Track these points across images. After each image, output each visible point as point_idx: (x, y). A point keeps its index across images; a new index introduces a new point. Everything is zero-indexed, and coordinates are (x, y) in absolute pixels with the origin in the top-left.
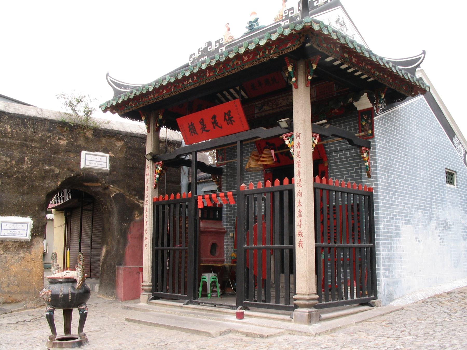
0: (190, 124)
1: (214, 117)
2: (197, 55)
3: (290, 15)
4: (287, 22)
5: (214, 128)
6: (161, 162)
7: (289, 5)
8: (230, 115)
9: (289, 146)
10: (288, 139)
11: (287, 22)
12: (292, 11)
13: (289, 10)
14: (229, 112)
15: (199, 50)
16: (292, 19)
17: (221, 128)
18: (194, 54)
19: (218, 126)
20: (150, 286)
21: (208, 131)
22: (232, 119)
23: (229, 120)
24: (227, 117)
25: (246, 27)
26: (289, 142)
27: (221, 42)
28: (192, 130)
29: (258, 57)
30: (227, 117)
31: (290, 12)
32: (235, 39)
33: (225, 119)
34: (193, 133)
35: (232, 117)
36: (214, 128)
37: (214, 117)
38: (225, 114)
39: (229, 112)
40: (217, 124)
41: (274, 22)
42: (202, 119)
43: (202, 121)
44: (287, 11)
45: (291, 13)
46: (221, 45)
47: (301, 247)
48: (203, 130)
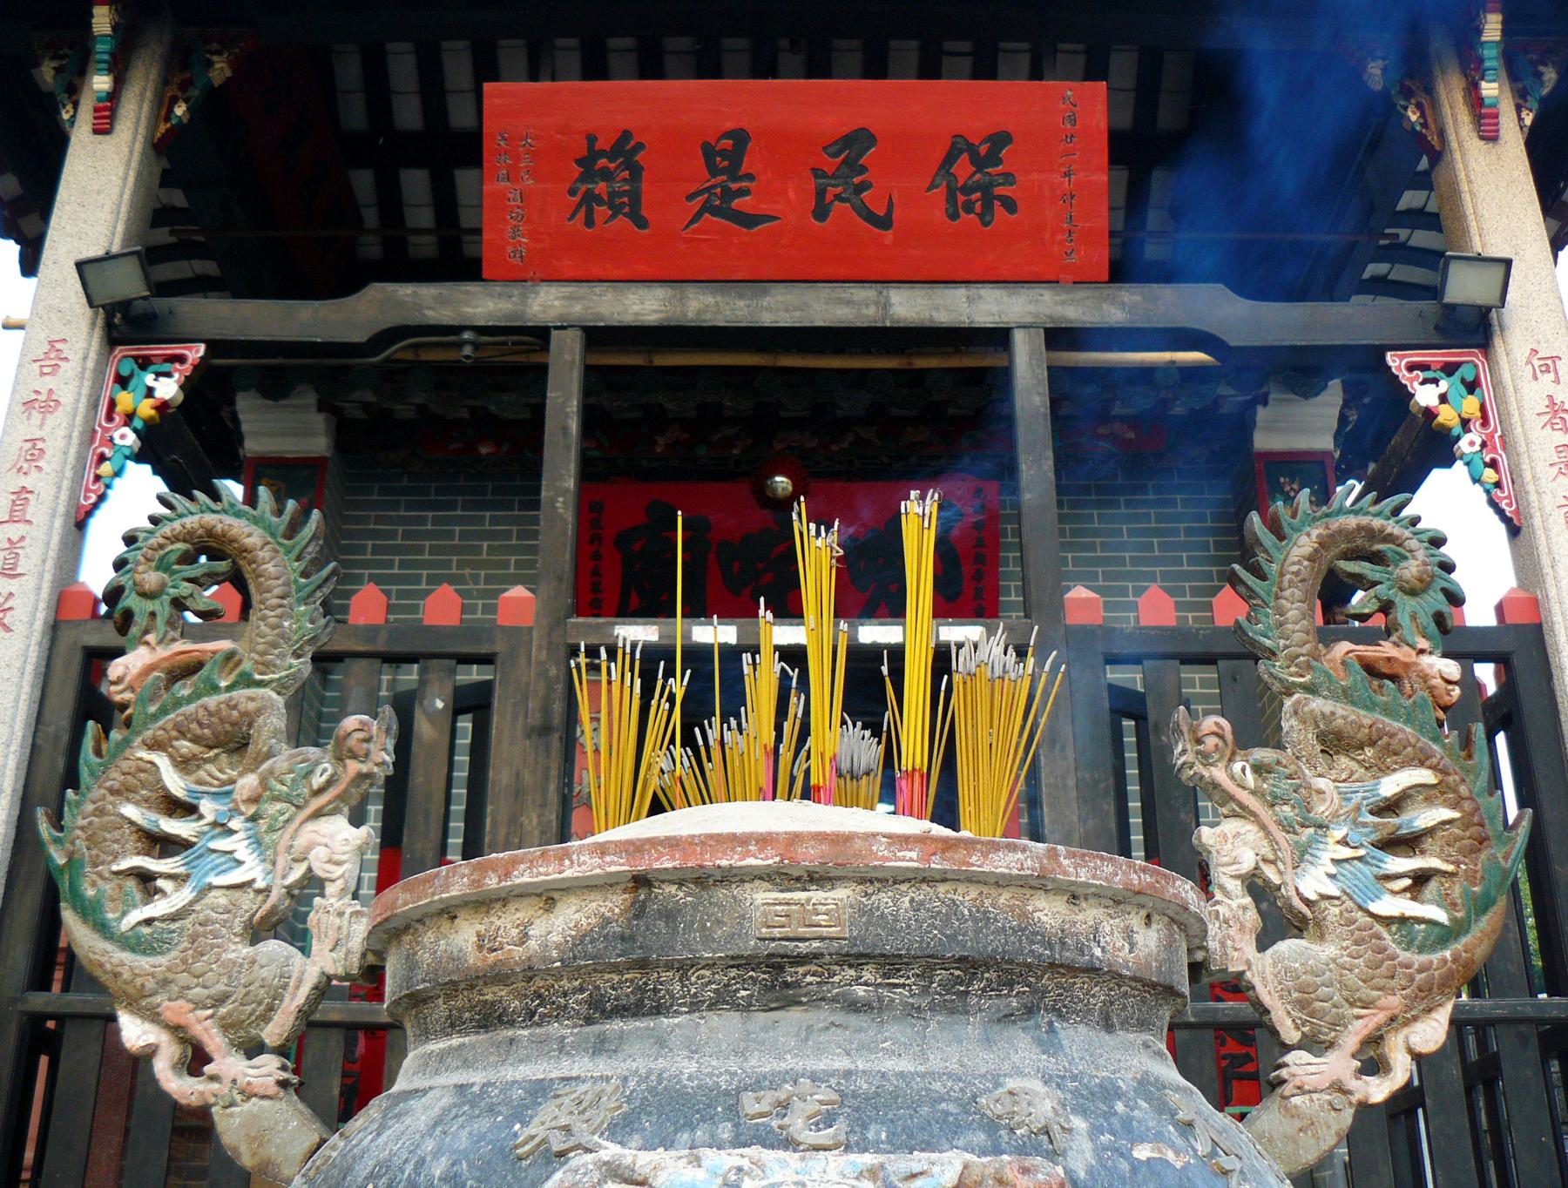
0: (602, 144)
5: (821, 213)
6: (196, 352)
8: (993, 158)
9: (1447, 416)
10: (1435, 381)
14: (1000, 139)
17: (884, 223)
26: (1443, 398)
34: (601, 210)
35: (1008, 177)
36: (821, 213)
37: (856, 141)
39: (1000, 139)
42: (740, 137)
43: (727, 143)
48: (706, 208)
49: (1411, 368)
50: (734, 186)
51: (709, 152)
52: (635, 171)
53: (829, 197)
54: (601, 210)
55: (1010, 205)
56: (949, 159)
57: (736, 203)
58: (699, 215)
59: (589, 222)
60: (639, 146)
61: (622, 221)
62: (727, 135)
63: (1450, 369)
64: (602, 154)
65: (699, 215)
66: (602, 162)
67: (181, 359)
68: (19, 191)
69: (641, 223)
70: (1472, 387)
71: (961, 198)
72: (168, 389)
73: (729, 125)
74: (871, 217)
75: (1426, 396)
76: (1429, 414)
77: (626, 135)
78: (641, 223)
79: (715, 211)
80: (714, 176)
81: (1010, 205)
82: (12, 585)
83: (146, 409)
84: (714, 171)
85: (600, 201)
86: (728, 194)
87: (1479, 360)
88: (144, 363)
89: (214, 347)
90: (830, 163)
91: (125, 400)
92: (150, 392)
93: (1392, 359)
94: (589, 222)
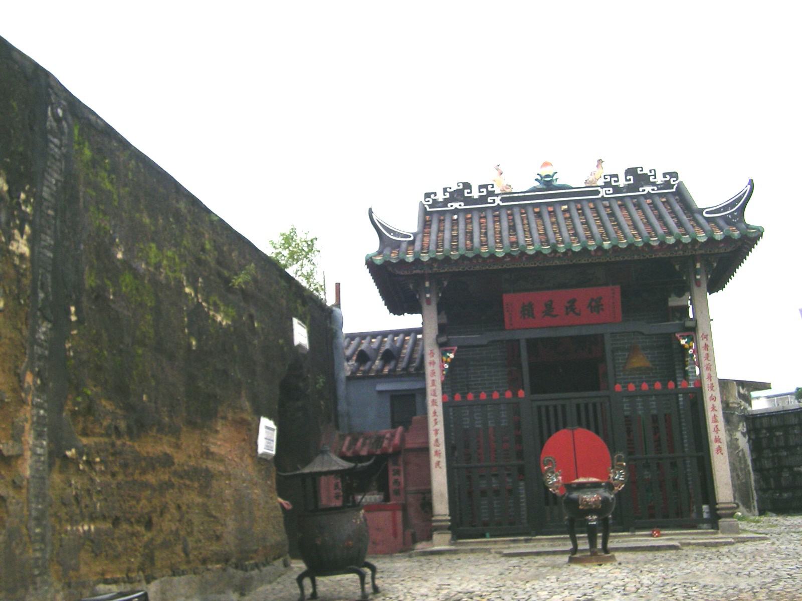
1: (573, 301)
2: (440, 197)
3: (613, 183)
4: (609, 191)
5: (567, 314)
6: (456, 348)
7: (608, 169)
9: (687, 346)
11: (609, 191)
12: (616, 179)
13: (612, 176)
15: (445, 190)
16: (617, 189)
18: (435, 194)
20: (449, 521)
24: (594, 304)
25: (536, 180)
26: (686, 342)
27: (490, 189)
28: (526, 312)
29: (676, 248)
30: (594, 304)
31: (613, 179)
32: (513, 191)
35: (602, 305)
36: (567, 314)
38: (593, 299)
39: (601, 298)
41: (584, 186)
44: (608, 177)
45: (615, 181)
46: (491, 194)
47: (720, 454)
49: (680, 336)
51: (546, 305)
54: (526, 316)
55: (602, 309)
63: (688, 336)
67: (453, 350)
70: (692, 340)
72: (452, 356)
74: (577, 314)
75: (683, 342)
76: (683, 346)
78: (534, 318)
81: (602, 309)
82: (436, 398)
83: (449, 360)
87: (694, 335)
88: (447, 351)
89: (459, 347)
91: (445, 359)
92: (449, 357)
93: (677, 335)
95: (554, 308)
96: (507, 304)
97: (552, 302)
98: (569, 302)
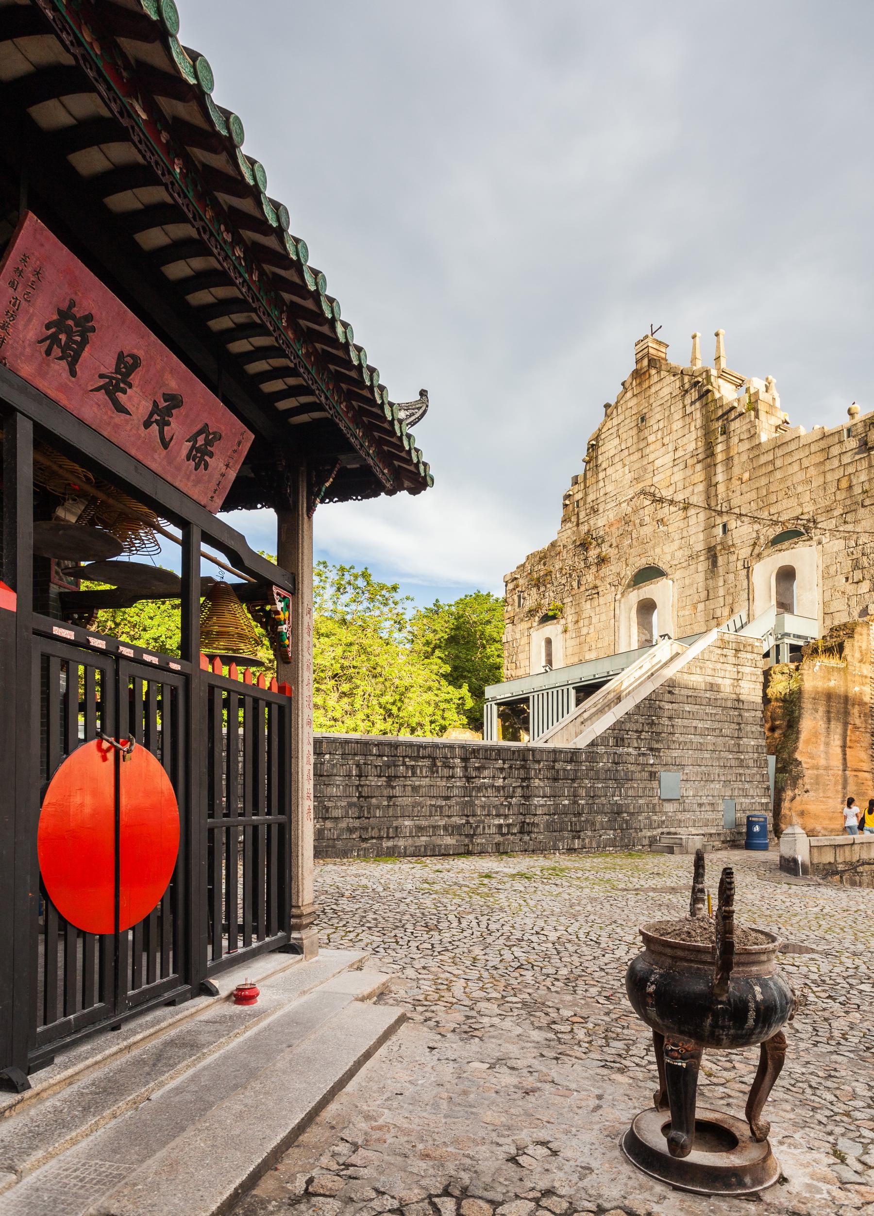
0: (79, 312)
1: (174, 401)
5: (147, 424)
17: (165, 444)
19: (161, 432)
21: (121, 409)
22: (206, 458)
23: (198, 450)
28: (63, 337)
33: (194, 438)
34: (57, 351)
35: (211, 455)
36: (147, 424)
37: (174, 401)
38: (204, 430)
39: (218, 437)
40: (163, 424)
42: (136, 362)
50: (122, 385)
52: (85, 342)
53: (153, 420)
54: (57, 351)
56: (199, 433)
57: (119, 395)
58: (97, 389)
59: (48, 352)
60: (93, 329)
61: (64, 363)
62: (133, 356)
64: (74, 318)
65: (97, 389)
66: (70, 322)
68: (163, 269)
69: (73, 373)
71: (194, 453)
73: (135, 352)
77: (89, 317)
78: (73, 373)
79: (108, 393)
80: (116, 373)
84: (118, 370)
85: (60, 346)
86: (118, 389)
90: (163, 404)
94: (48, 352)
95: (130, 386)
96: (25, 259)
97: (136, 362)
98: (167, 397)
